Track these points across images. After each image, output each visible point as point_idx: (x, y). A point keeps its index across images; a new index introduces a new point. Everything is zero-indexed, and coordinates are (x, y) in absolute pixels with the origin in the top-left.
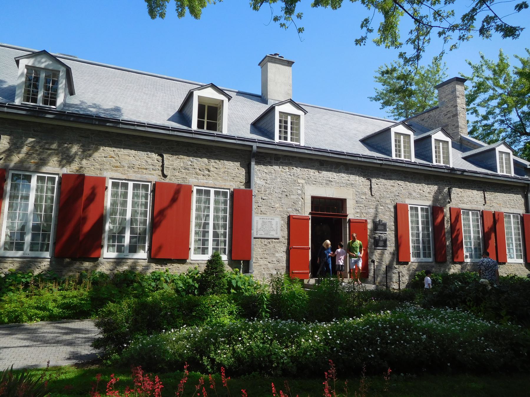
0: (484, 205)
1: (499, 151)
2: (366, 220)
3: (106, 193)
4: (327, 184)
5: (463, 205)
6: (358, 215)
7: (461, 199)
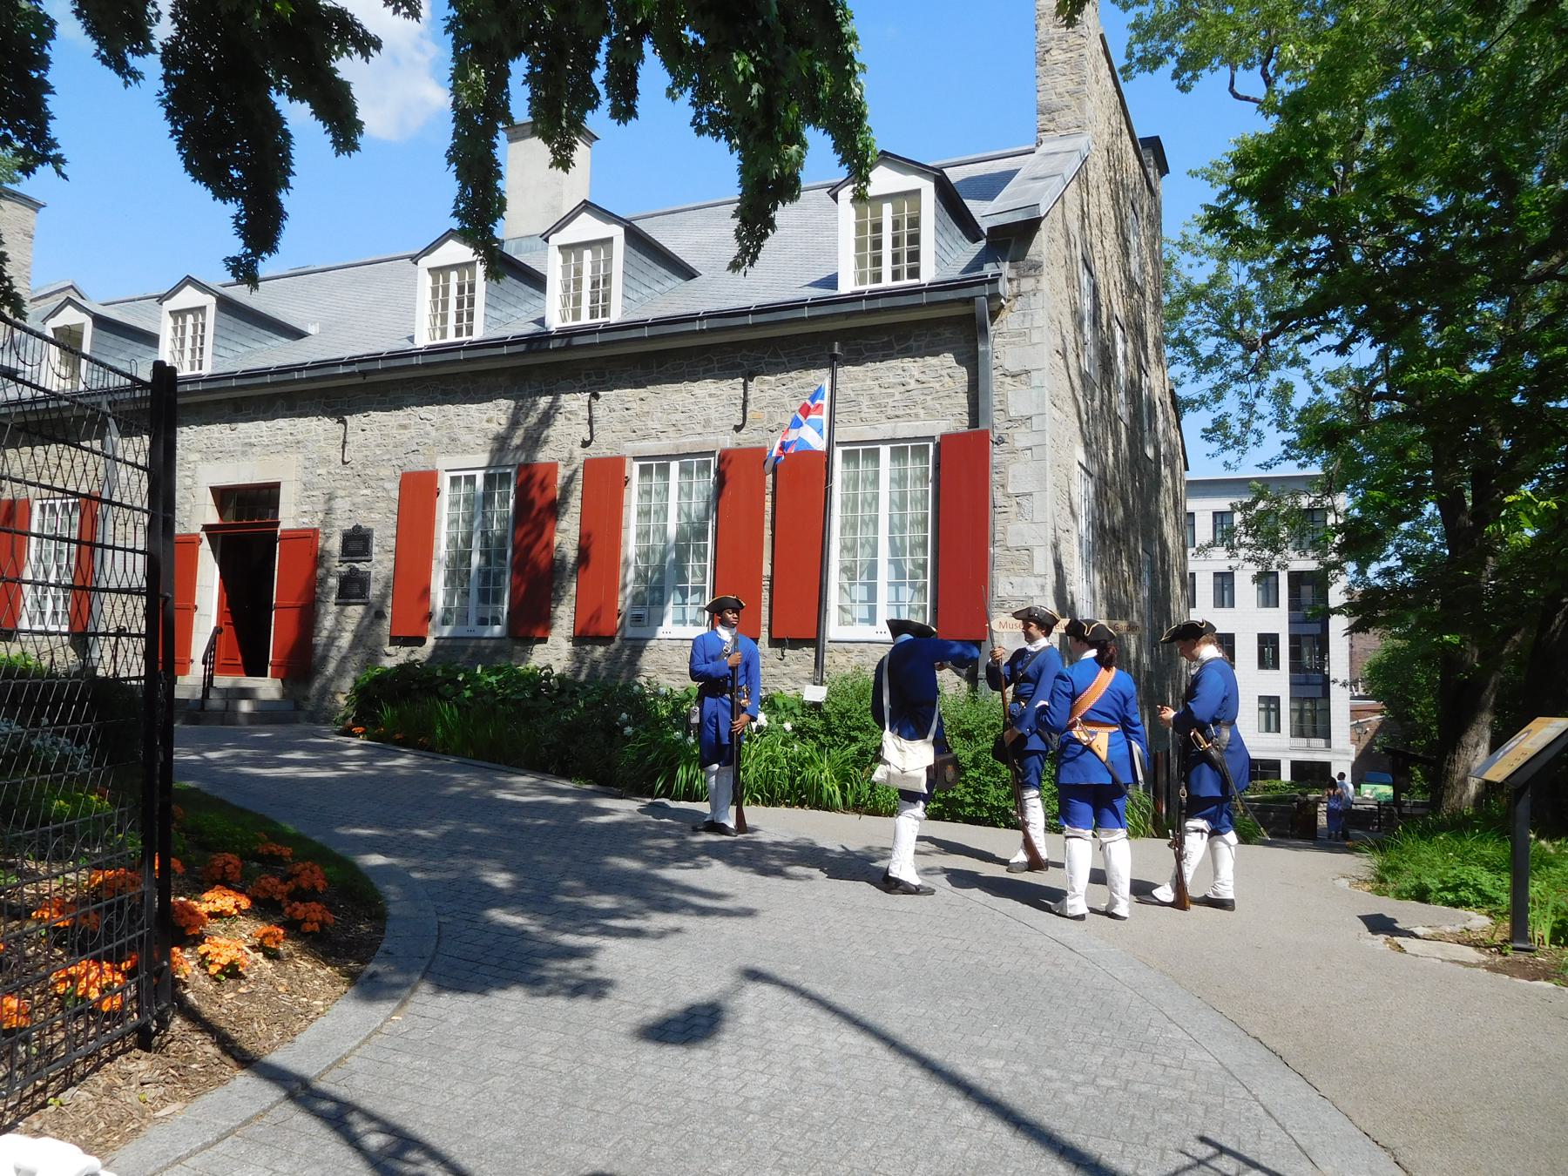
0: (738, 429)
1: (429, 270)
3: (626, 491)
4: (244, 453)
5: (645, 443)
6: (306, 520)
7: (636, 424)
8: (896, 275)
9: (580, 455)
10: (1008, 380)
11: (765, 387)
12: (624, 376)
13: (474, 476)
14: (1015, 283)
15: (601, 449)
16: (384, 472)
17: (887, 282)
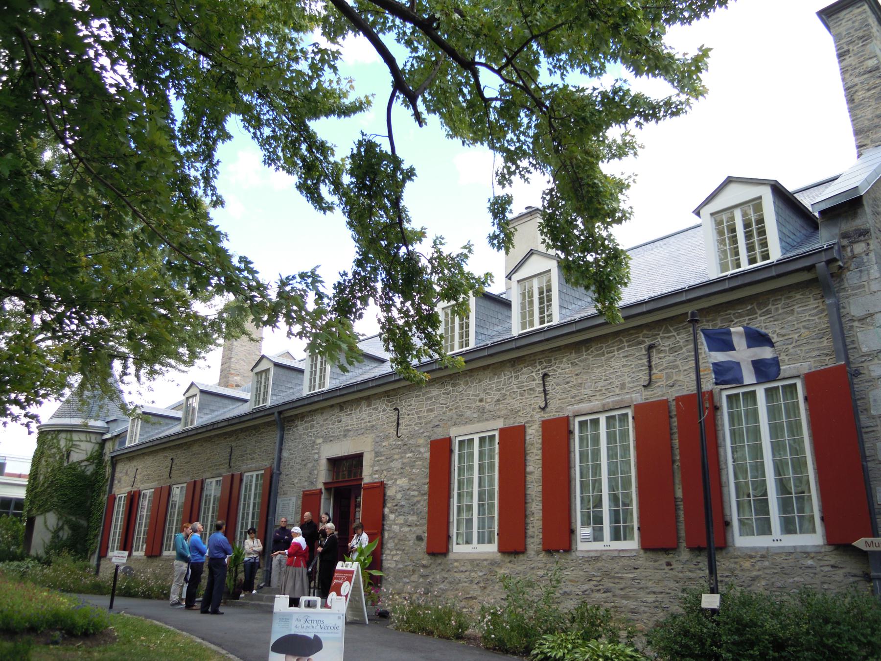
2: (382, 483)
4: (345, 436)
6: (377, 476)
8: (752, 261)
9: (539, 417)
10: (856, 324)
11: (662, 355)
12: (565, 360)
13: (473, 440)
14: (849, 249)
15: (552, 414)
16: (421, 441)
17: (745, 266)
